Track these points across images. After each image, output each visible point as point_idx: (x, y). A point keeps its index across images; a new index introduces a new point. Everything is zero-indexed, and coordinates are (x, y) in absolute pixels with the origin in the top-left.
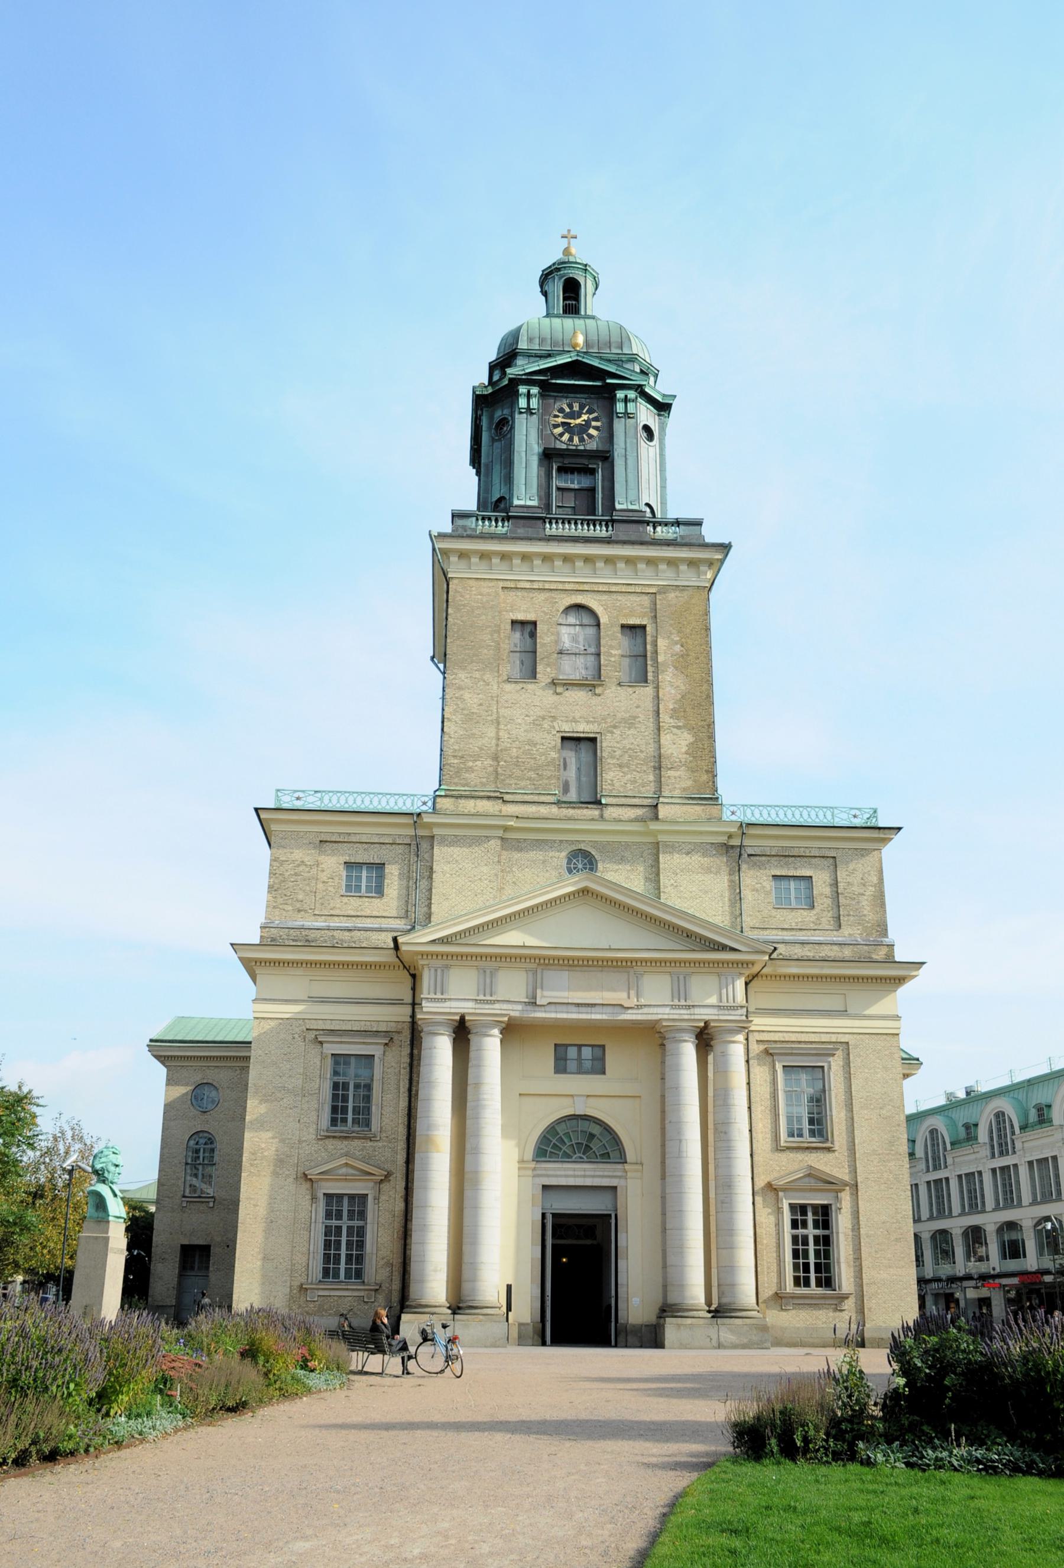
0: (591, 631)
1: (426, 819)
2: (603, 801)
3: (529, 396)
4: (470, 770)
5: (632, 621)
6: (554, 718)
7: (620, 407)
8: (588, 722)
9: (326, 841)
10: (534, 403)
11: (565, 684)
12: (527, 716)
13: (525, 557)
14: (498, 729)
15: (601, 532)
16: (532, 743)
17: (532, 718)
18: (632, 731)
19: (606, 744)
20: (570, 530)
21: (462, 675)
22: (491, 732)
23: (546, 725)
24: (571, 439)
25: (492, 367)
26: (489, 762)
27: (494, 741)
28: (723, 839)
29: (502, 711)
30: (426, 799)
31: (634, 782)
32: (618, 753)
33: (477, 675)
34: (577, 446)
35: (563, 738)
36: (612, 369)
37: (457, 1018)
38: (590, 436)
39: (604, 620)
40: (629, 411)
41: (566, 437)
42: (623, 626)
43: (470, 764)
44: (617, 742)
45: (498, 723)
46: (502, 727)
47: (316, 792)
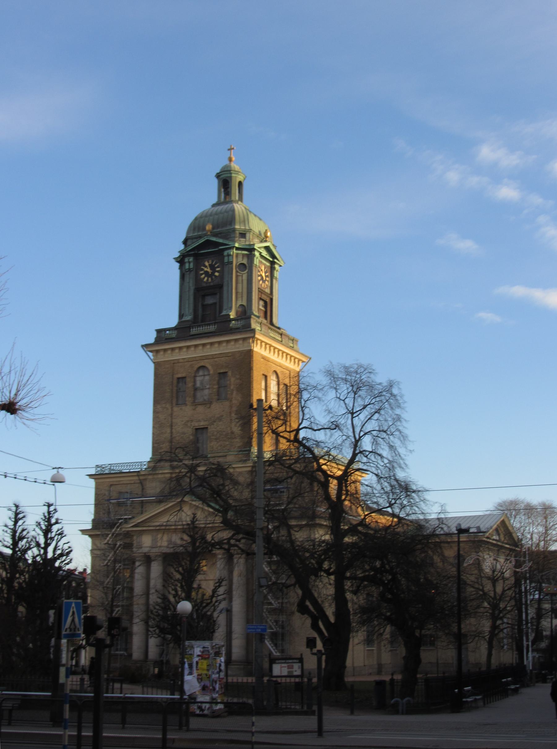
0: (207, 378)
1: (142, 473)
2: (209, 456)
3: (189, 262)
4: (161, 448)
5: (222, 371)
6: (192, 421)
7: (226, 260)
8: (205, 421)
9: (113, 485)
10: (192, 266)
11: (196, 405)
12: (182, 421)
13: (180, 348)
14: (172, 429)
15: (212, 328)
16: (184, 433)
17: (184, 422)
18: (221, 423)
19: (211, 429)
20: (201, 330)
21: (159, 406)
22: (168, 430)
23: (189, 425)
24: (208, 280)
25: (185, 242)
26: (167, 444)
27: (170, 435)
28: (249, 469)
29: (174, 421)
30: (145, 463)
31: (221, 446)
32: (215, 433)
33: (164, 405)
34: (210, 283)
35: (197, 429)
36: (221, 241)
37: (143, 554)
38: (216, 276)
39: (211, 372)
40: (230, 261)
41: (206, 279)
42: (220, 373)
43: (162, 446)
44: (215, 428)
45: (171, 426)
46: (173, 427)
47: (109, 464)
